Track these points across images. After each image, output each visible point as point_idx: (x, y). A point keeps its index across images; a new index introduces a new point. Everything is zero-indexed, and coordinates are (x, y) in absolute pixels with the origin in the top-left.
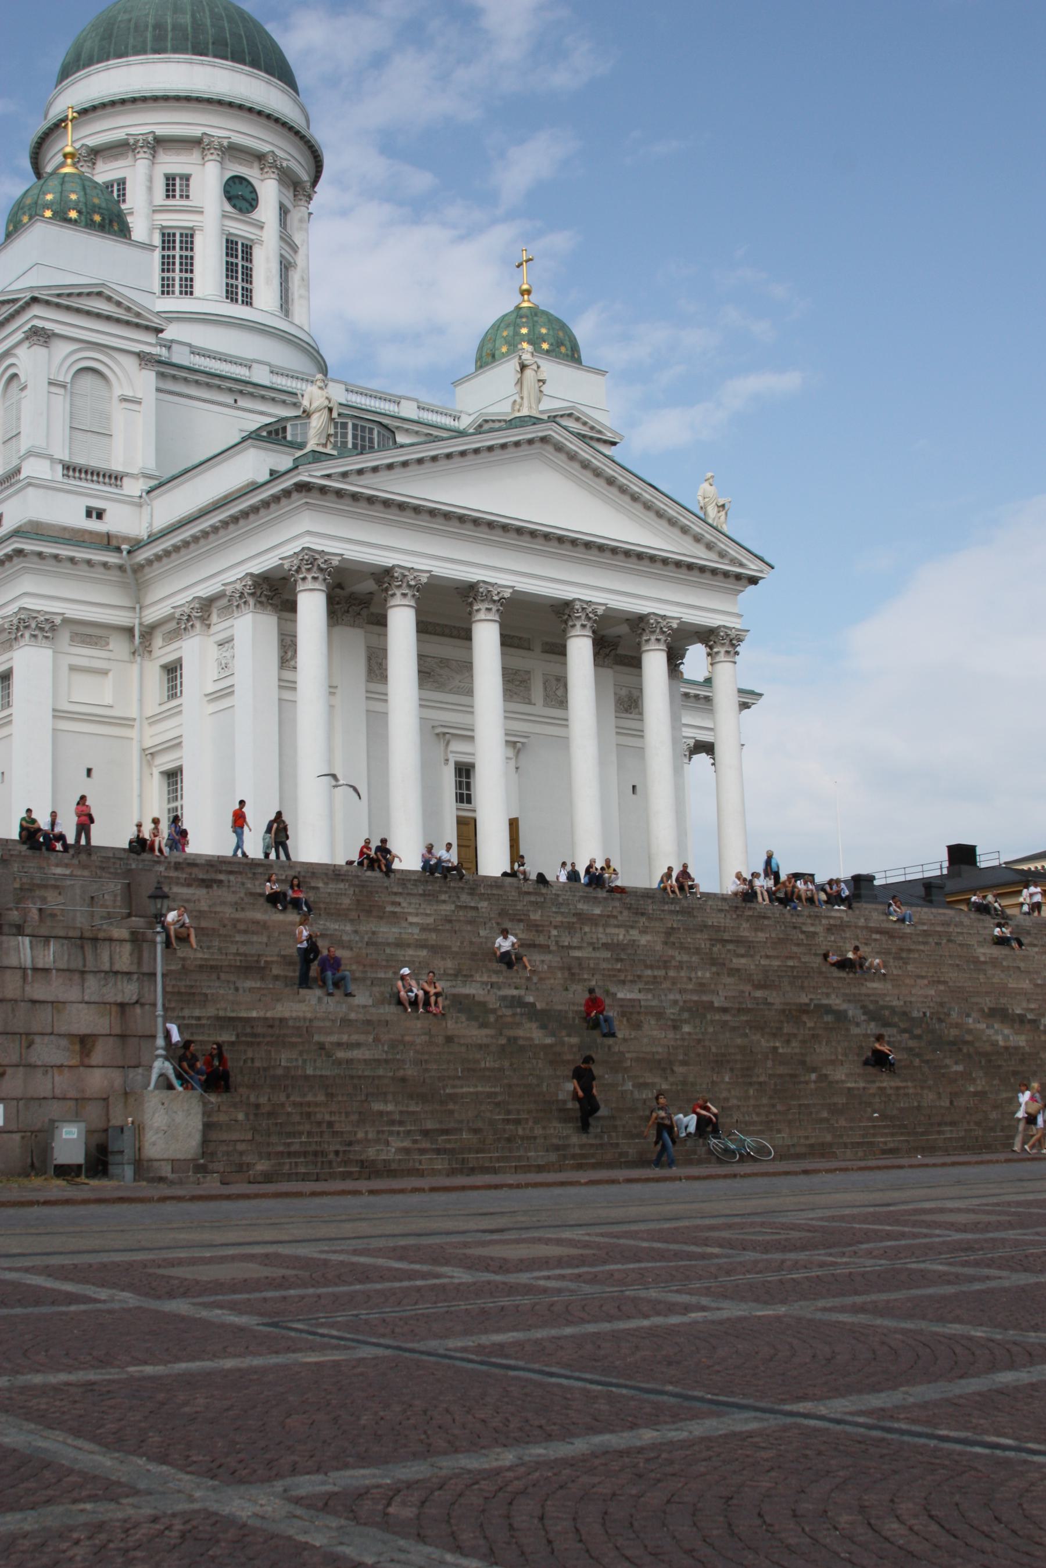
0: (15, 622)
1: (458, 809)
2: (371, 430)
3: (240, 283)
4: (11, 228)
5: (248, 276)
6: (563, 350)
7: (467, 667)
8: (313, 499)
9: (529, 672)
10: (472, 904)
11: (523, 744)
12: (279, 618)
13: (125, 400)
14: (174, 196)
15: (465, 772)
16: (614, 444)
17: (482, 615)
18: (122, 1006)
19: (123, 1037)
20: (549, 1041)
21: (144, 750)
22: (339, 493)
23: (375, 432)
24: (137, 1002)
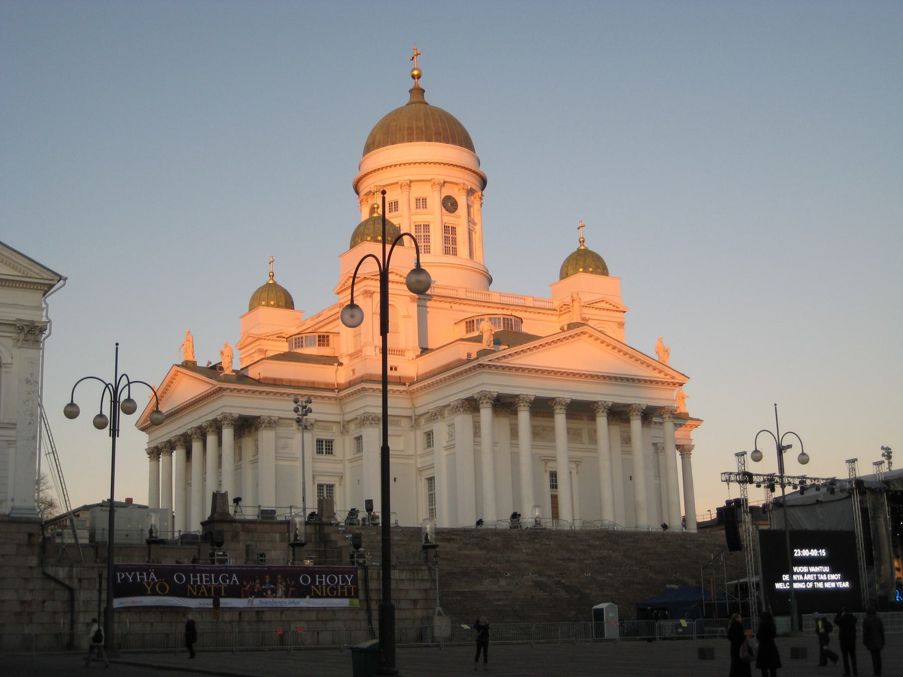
0: (363, 418)
1: (551, 491)
2: (511, 320)
3: (451, 246)
4: (353, 243)
5: (454, 241)
6: (599, 270)
7: (553, 429)
8: (486, 370)
9: (580, 429)
10: (548, 543)
11: (579, 461)
12: (473, 416)
13: (405, 317)
14: (420, 208)
15: (554, 475)
16: (625, 312)
17: (557, 411)
18: (426, 590)
19: (426, 599)
20: (568, 596)
21: (418, 469)
22: (497, 367)
23: (513, 321)
24: (430, 589)
